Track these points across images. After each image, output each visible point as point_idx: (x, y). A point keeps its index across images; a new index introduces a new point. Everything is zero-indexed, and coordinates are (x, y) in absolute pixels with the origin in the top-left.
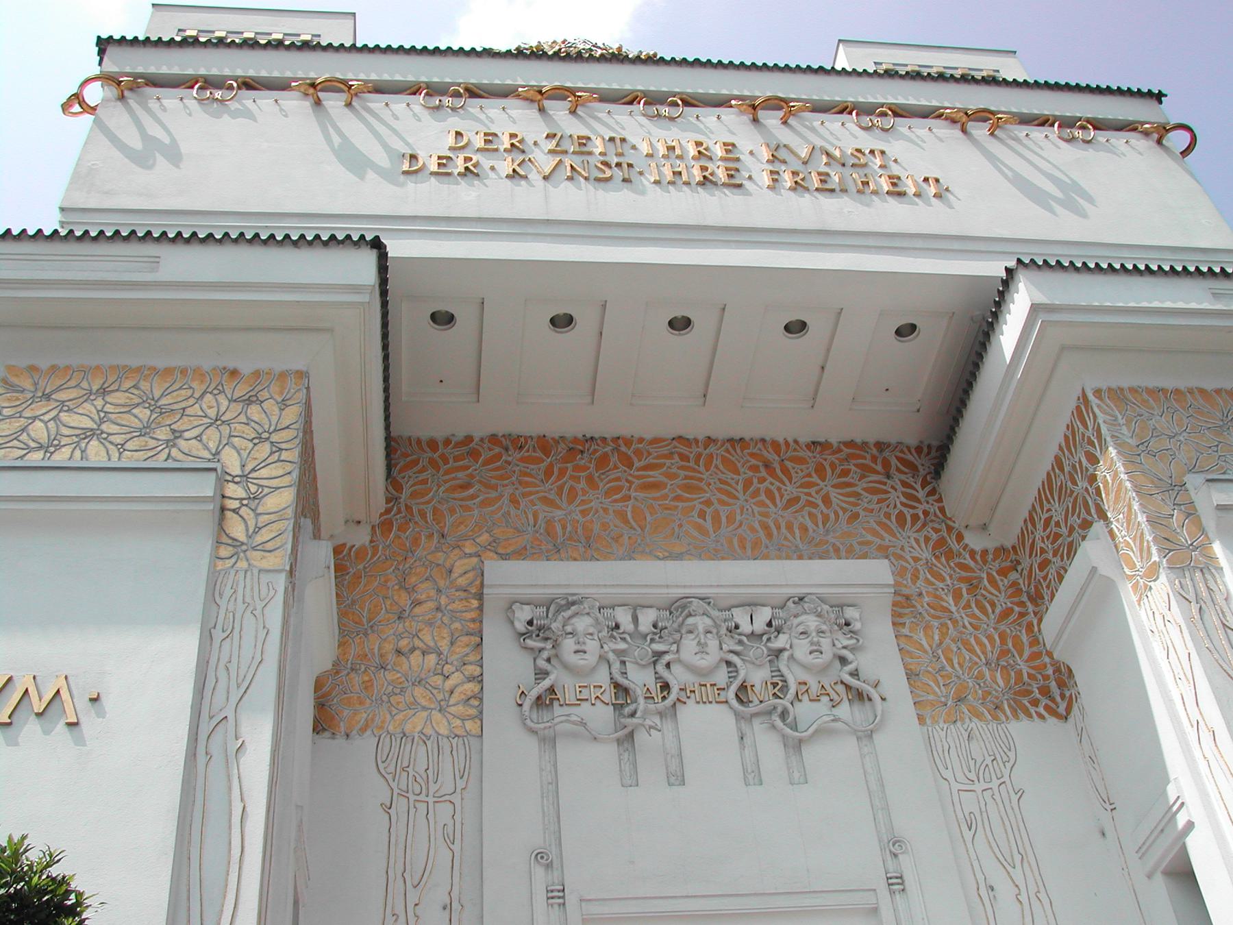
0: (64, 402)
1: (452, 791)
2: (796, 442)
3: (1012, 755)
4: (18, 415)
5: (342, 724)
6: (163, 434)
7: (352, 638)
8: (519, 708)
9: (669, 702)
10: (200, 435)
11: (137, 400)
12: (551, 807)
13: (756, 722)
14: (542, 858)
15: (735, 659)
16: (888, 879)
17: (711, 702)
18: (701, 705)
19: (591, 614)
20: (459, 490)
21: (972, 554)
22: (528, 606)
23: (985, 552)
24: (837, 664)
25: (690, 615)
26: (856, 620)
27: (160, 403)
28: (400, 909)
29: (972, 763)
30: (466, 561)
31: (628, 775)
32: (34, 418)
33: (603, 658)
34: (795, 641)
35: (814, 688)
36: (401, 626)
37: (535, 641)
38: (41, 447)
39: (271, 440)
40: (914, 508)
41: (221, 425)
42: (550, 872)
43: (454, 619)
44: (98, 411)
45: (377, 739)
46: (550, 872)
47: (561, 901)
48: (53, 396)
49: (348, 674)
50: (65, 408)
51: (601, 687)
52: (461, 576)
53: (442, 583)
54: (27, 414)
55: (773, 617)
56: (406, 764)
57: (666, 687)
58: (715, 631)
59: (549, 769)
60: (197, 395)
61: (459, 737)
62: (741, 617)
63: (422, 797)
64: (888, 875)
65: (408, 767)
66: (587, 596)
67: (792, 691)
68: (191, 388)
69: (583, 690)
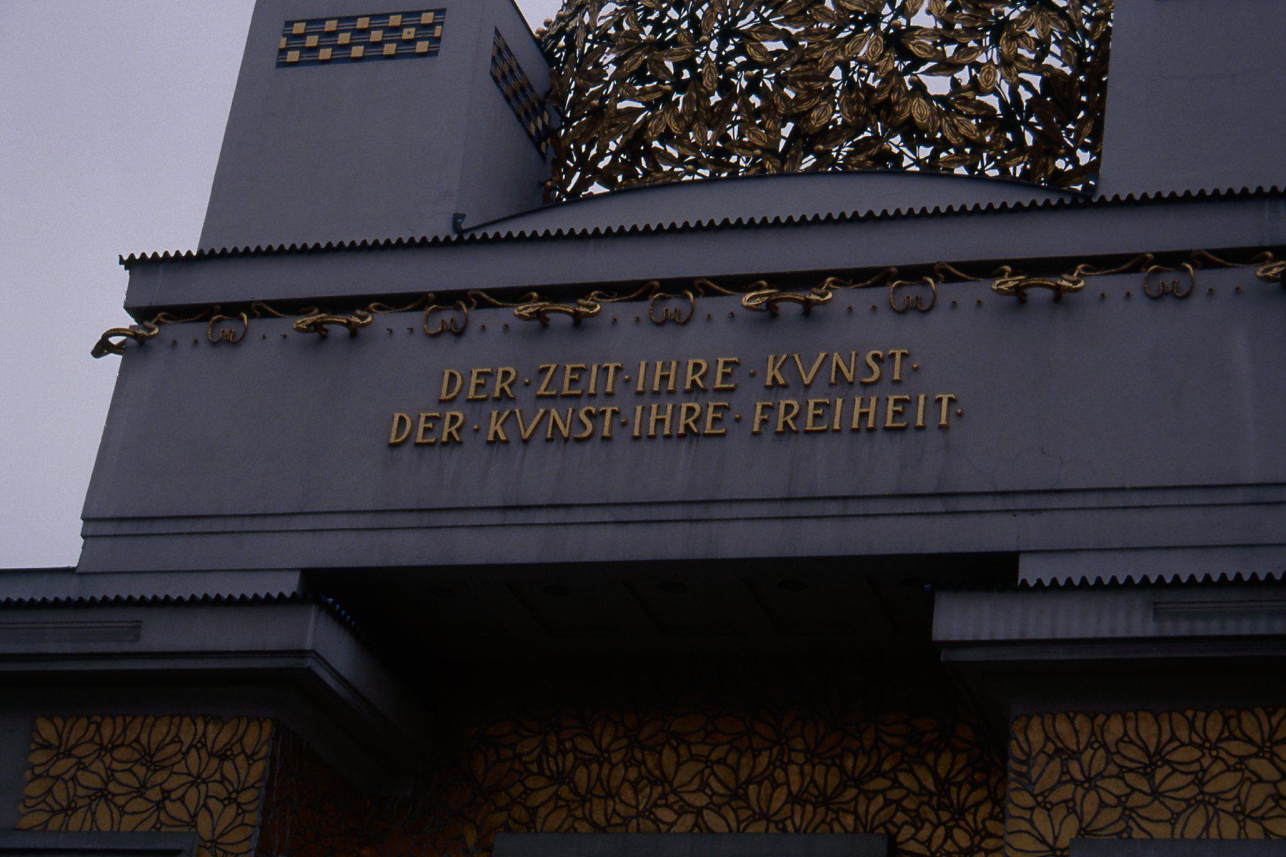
0: (80, 758)
4: (45, 774)
6: (155, 794)
10: (183, 796)
11: (137, 756)
27: (156, 759)
32: (58, 778)
38: (63, 810)
39: (239, 800)
41: (200, 784)
44: (107, 769)
48: (73, 752)
50: (82, 766)
54: (52, 772)
60: (184, 749)
68: (181, 742)
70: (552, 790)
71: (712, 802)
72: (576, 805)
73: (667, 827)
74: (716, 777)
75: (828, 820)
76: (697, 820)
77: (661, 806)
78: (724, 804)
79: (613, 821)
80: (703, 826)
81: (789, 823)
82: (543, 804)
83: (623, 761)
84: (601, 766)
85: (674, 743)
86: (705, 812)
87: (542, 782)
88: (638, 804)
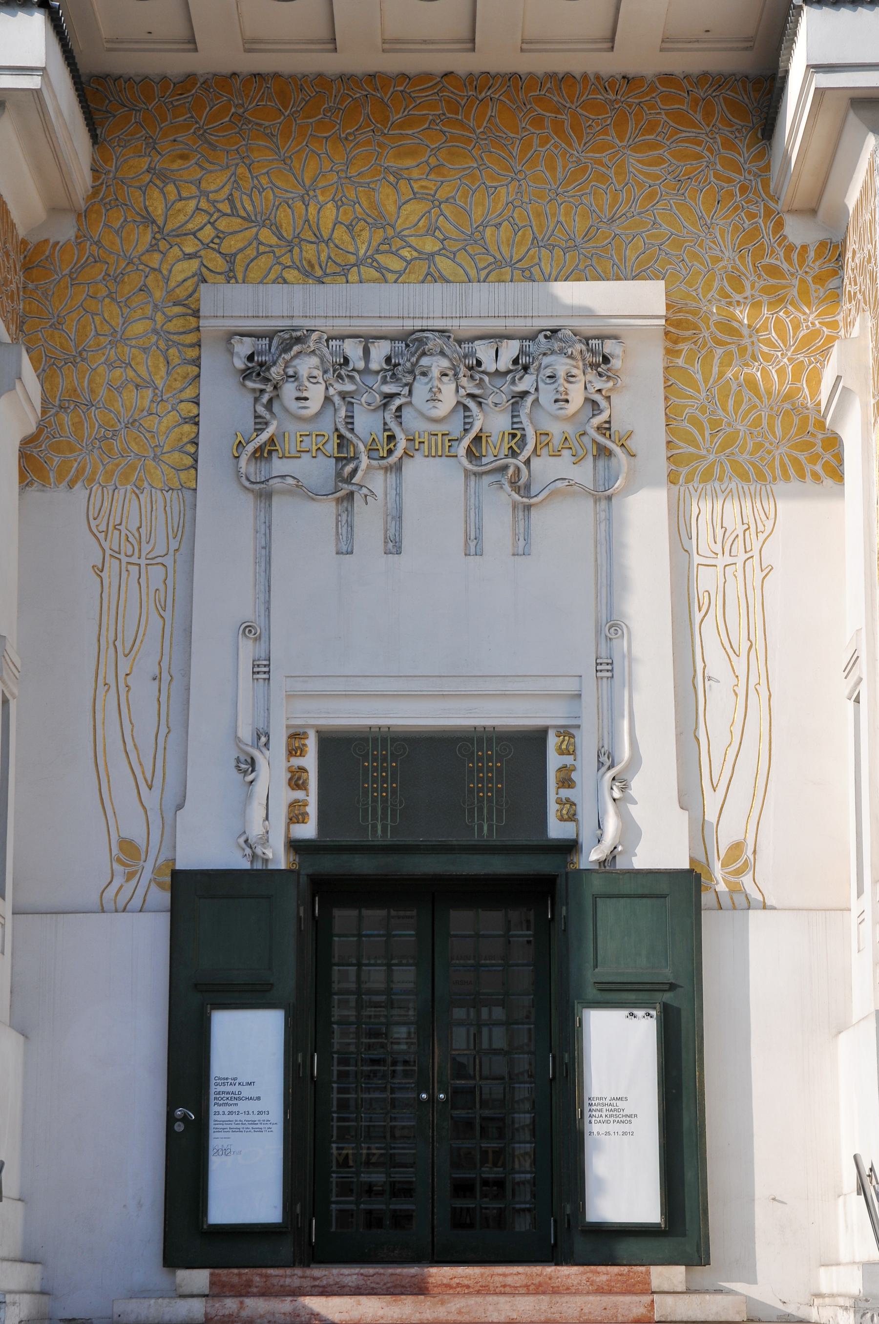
1: (165, 553)
2: (598, 77)
3: (769, 524)
5: (51, 475)
7: (60, 368)
8: (235, 461)
9: (393, 459)
12: (263, 574)
13: (487, 480)
14: (250, 631)
15: (472, 404)
16: (597, 664)
17: (441, 456)
18: (431, 459)
19: (317, 352)
20: (180, 161)
21: (790, 248)
22: (249, 339)
23: (804, 248)
24: (589, 407)
25: (424, 354)
26: (618, 356)
28: (111, 680)
29: (719, 532)
30: (185, 264)
31: (345, 539)
33: (328, 399)
34: (541, 385)
35: (557, 441)
36: (113, 352)
37: (254, 381)
40: (729, 180)
42: (257, 644)
43: (170, 343)
45: (88, 491)
46: (257, 644)
47: (266, 676)
49: (56, 414)
51: (324, 435)
52: (178, 286)
53: (158, 294)
55: (522, 352)
56: (117, 522)
57: (391, 438)
58: (451, 373)
59: (263, 531)
61: (173, 489)
62: (484, 352)
63: (134, 560)
64: (598, 661)
65: (120, 524)
66: (314, 329)
67: (530, 447)
69: (304, 438)
70: (250, 234)
71: (444, 248)
72: (283, 251)
73: (395, 276)
74: (446, 217)
75: (581, 267)
76: (429, 268)
77: (387, 252)
78: (459, 250)
79: (328, 271)
80: (436, 275)
81: (536, 270)
82: (241, 250)
83: (333, 199)
84: (307, 206)
85: (391, 178)
86: (437, 258)
87: (236, 223)
88: (358, 250)
